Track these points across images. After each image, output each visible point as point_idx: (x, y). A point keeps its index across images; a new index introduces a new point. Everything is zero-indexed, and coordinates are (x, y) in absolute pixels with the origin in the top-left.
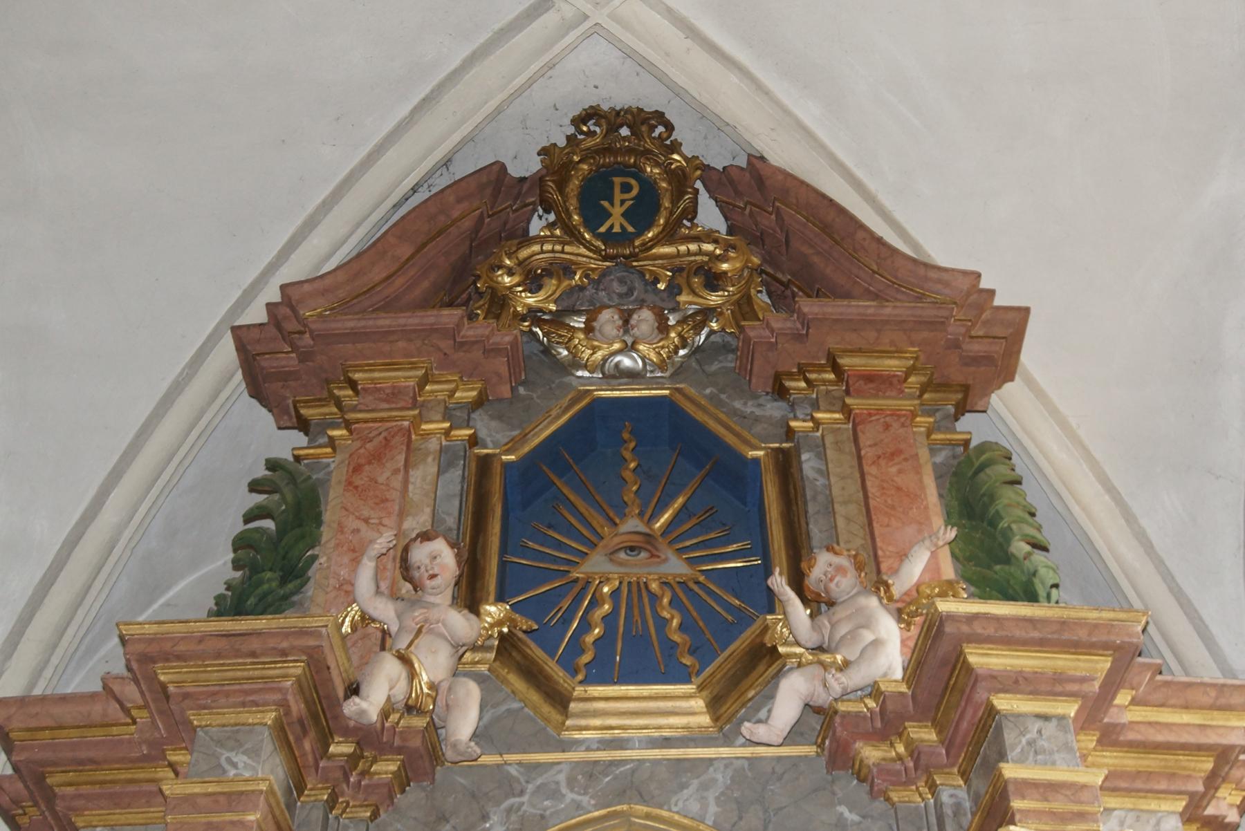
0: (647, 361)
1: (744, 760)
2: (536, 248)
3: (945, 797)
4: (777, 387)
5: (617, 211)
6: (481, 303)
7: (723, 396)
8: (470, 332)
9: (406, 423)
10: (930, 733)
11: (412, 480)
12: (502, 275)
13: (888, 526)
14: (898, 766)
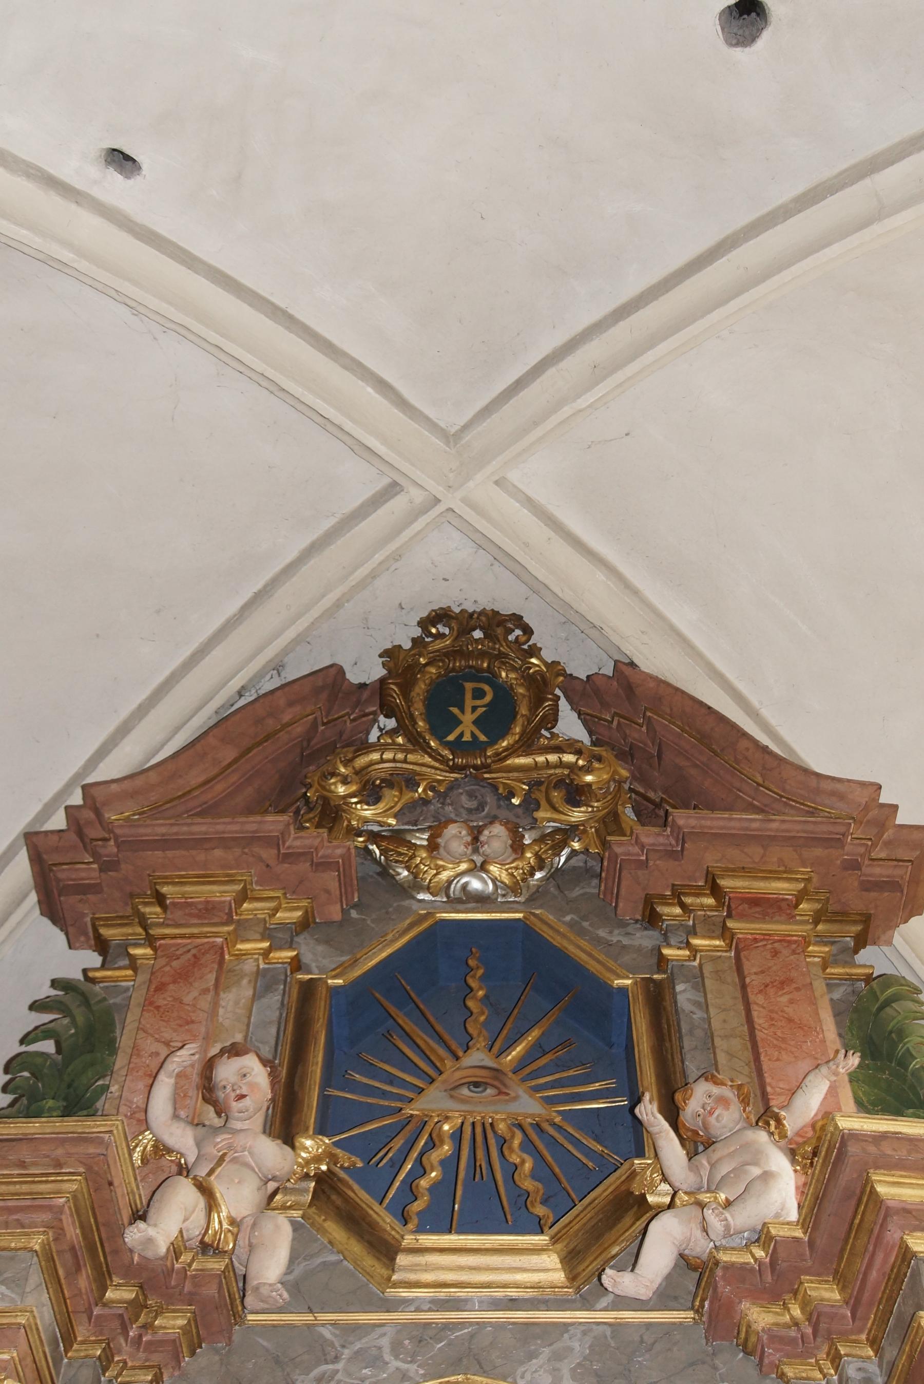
0: (499, 884)
1: (605, 1327)
2: (375, 756)
4: (647, 913)
5: (468, 718)
6: (311, 815)
7: (586, 924)
8: (295, 842)
9: (219, 940)
10: (832, 1290)
11: (223, 1003)
12: (335, 784)
13: (778, 1060)
14: (793, 1333)
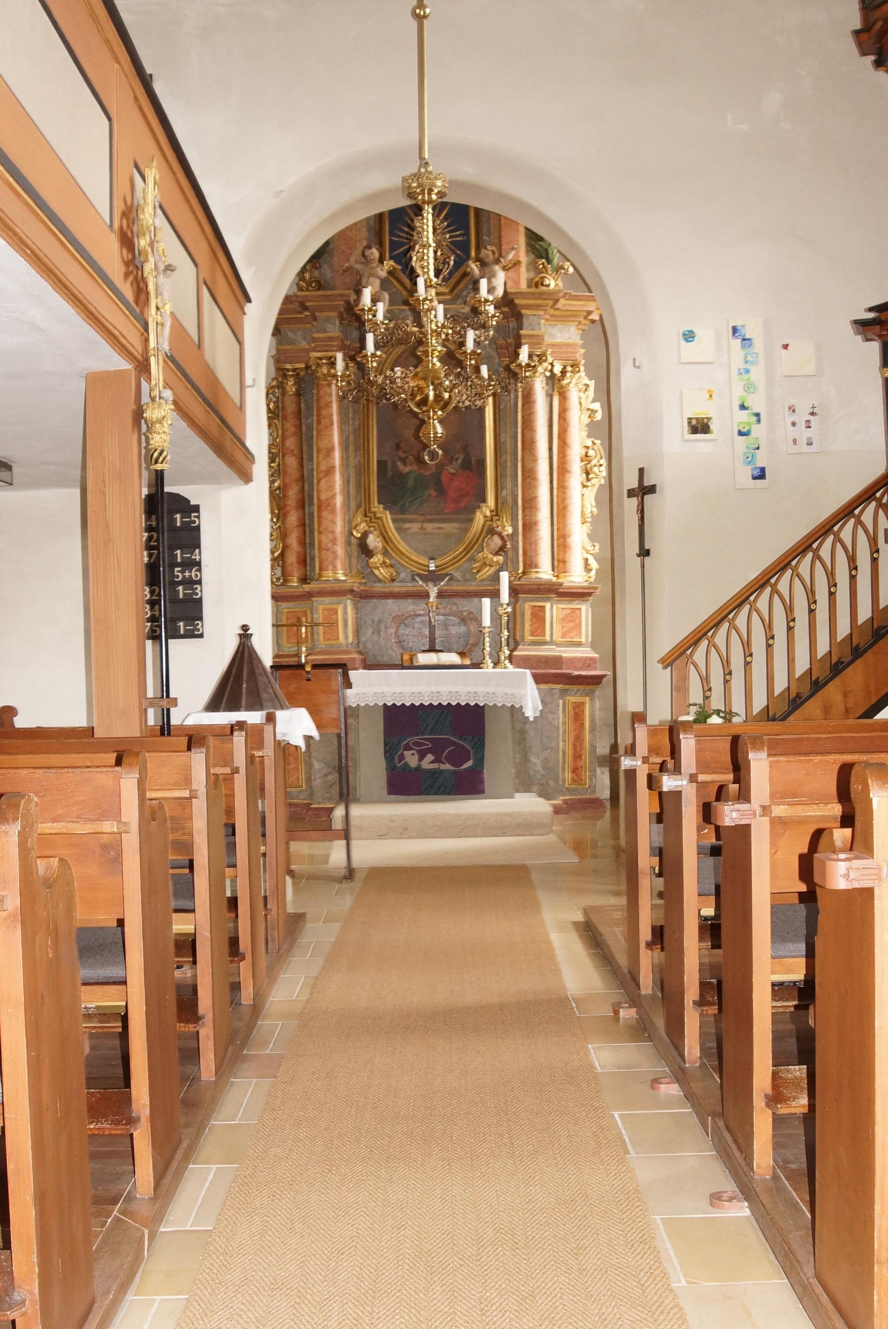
3: (511, 325)
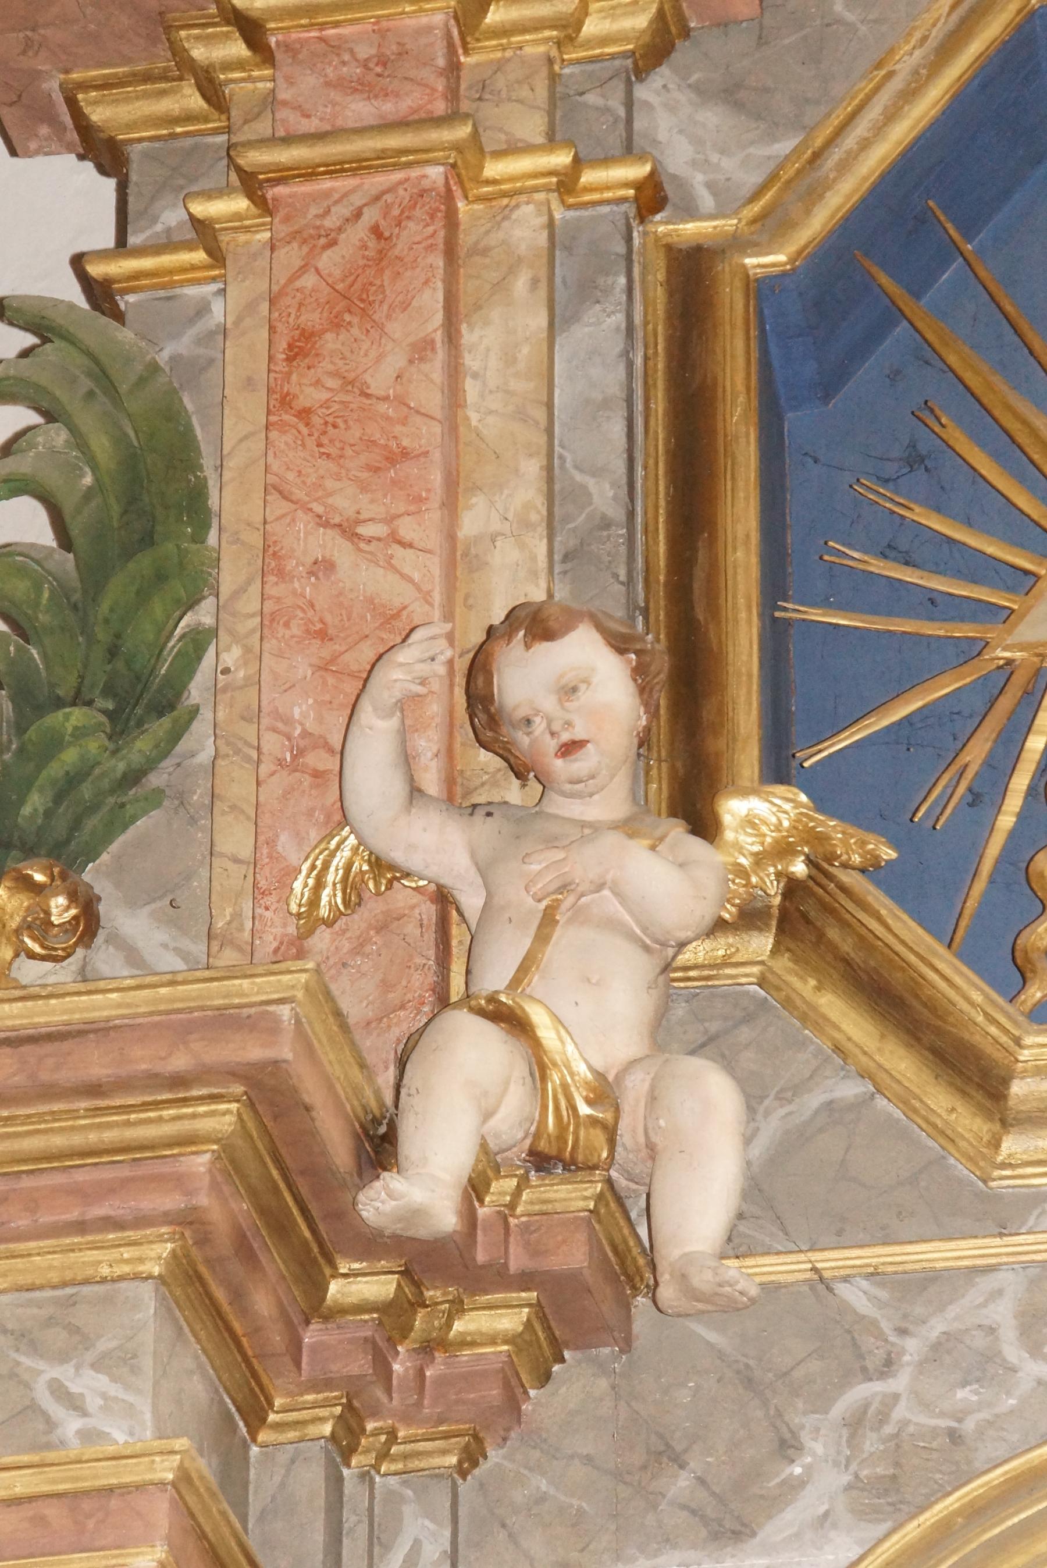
9: (435, 173)
